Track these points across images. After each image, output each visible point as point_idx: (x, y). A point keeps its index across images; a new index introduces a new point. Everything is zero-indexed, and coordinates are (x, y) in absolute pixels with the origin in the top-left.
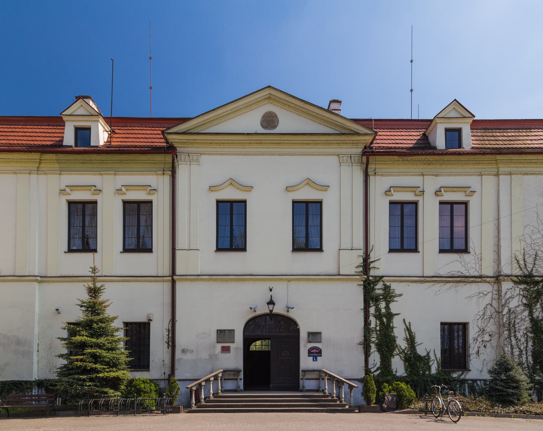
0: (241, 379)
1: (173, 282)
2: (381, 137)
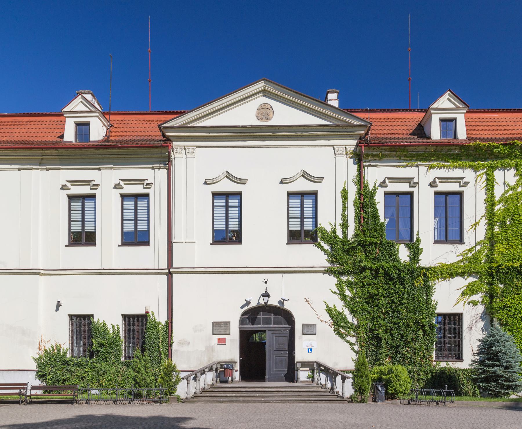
0: (236, 371)
1: (170, 275)
2: (377, 128)
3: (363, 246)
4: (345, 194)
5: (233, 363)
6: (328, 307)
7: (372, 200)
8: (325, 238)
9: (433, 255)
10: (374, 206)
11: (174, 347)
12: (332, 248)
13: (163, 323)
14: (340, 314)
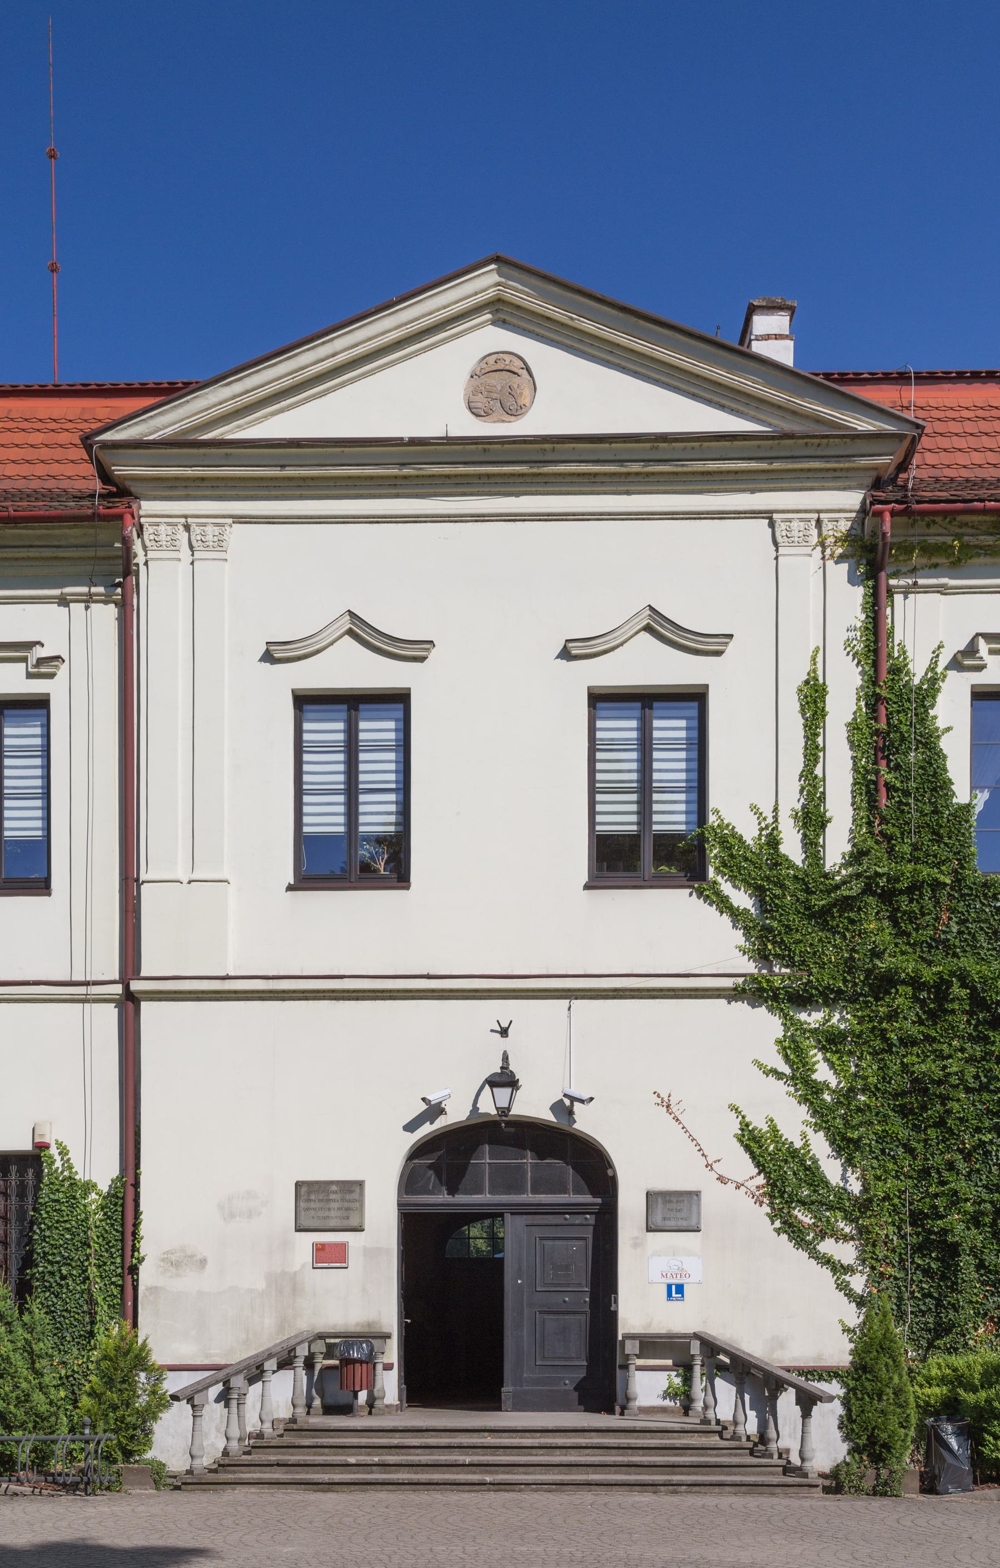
0: (388, 1367)
1: (129, 1003)
2: (944, 442)
3: (887, 896)
4: (813, 698)
5: (371, 1337)
6: (745, 1126)
7: (923, 717)
8: (739, 861)
10: (928, 742)
11: (147, 1276)
13: (104, 1187)
14: (793, 1153)
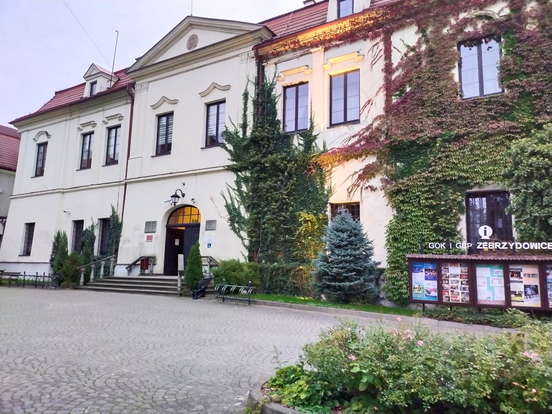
9: (330, 139)
12: (234, 149)
